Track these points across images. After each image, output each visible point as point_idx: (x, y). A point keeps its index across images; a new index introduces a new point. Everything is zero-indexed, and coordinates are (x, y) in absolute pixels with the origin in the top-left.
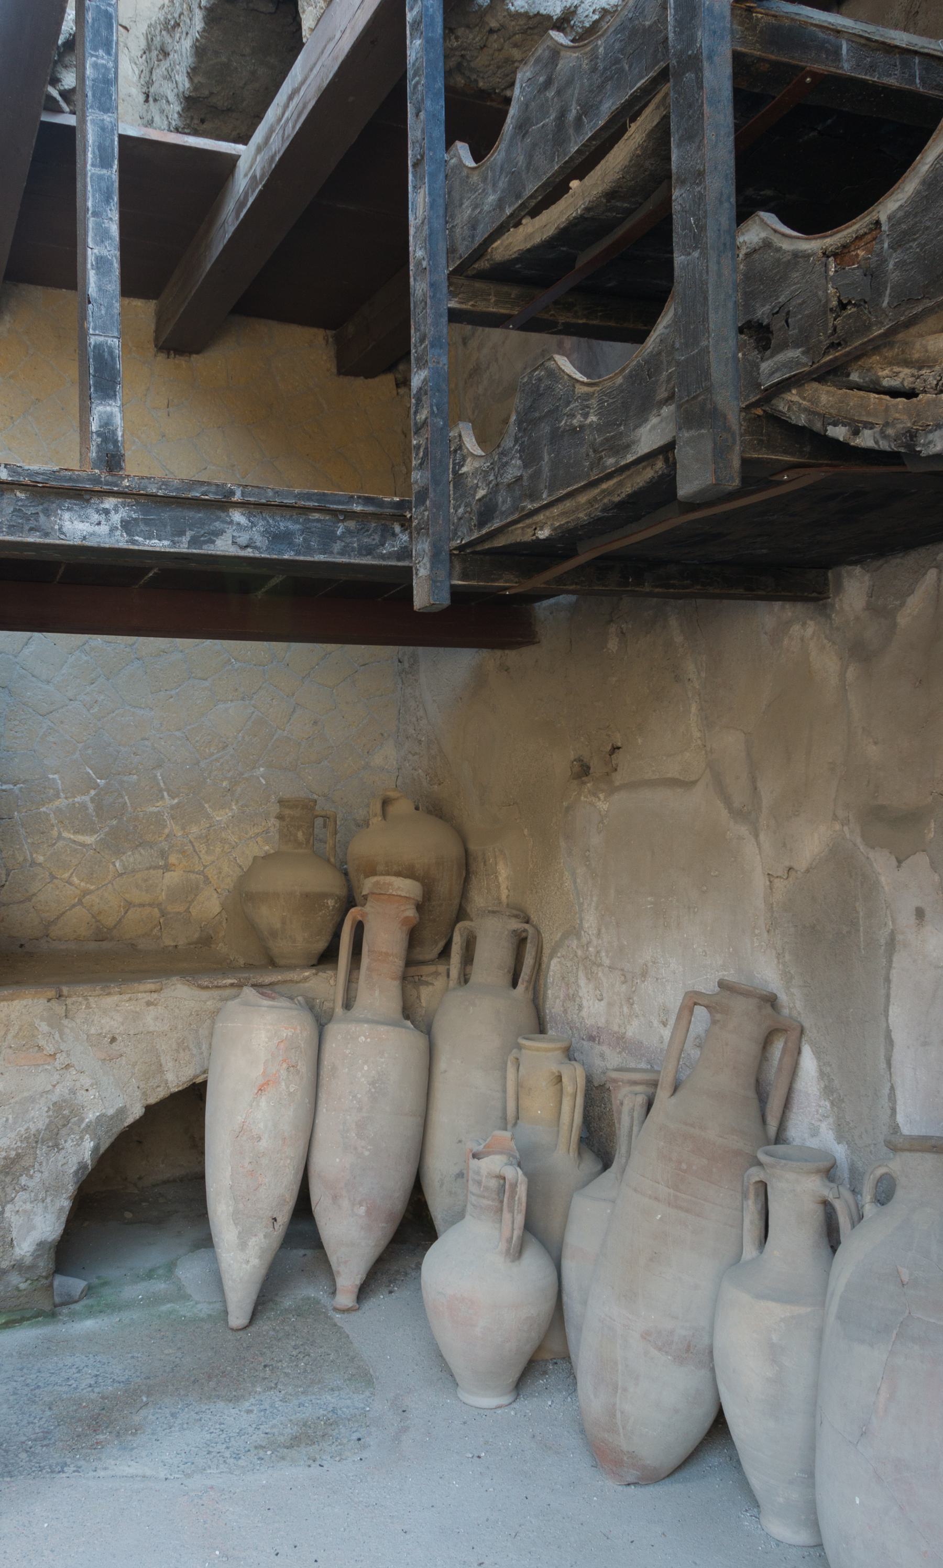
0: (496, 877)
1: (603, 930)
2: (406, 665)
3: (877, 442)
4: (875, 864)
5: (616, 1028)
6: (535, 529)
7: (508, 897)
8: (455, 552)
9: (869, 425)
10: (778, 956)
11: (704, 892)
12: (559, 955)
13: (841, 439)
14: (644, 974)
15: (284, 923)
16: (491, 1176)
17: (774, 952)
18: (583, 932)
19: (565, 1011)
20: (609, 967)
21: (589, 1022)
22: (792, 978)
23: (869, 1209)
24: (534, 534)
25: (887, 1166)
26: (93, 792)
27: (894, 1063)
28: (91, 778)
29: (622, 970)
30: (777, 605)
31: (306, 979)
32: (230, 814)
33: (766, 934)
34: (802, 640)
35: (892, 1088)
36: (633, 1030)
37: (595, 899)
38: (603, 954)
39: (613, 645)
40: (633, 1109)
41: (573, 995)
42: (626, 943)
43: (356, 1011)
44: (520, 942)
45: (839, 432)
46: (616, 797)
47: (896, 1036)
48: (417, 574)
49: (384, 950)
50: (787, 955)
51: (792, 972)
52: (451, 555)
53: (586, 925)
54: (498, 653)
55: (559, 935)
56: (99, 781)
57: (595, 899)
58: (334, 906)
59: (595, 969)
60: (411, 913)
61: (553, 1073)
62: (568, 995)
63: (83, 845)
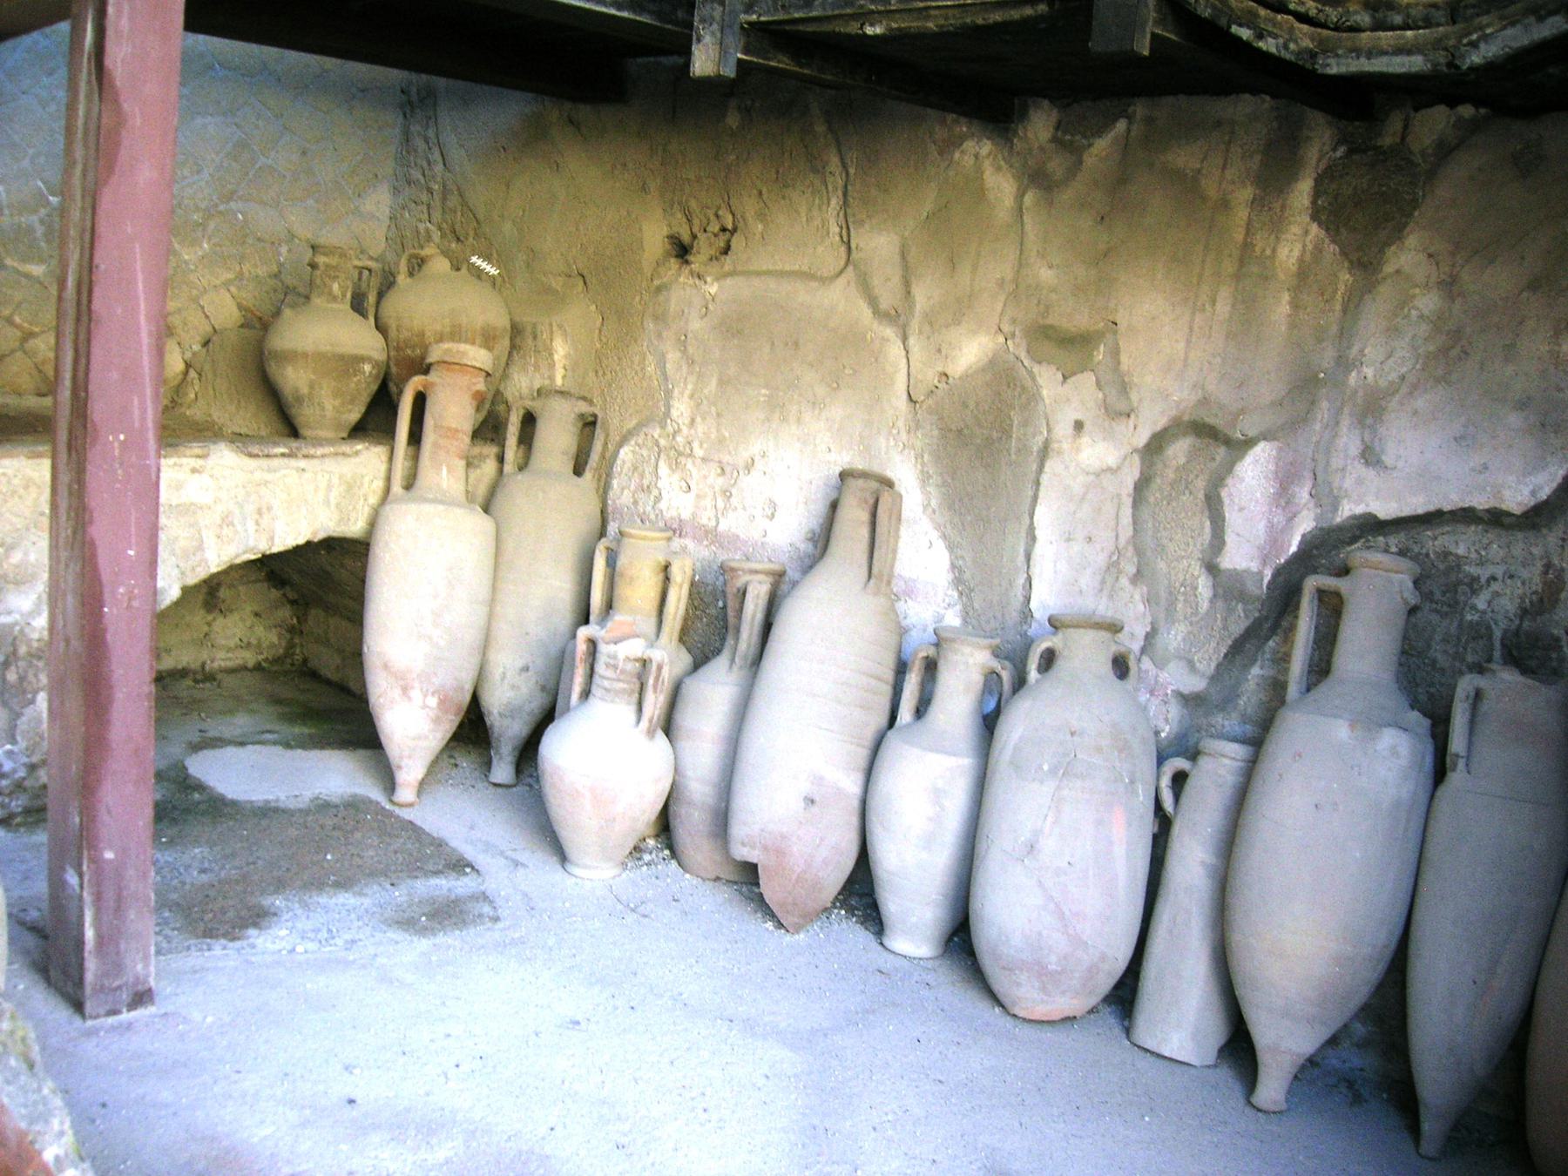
0: (551, 355)
1: (699, 419)
2: (414, 98)
3: (1279, 51)
4: (1038, 378)
5: (704, 521)
6: (862, 25)
7: (564, 377)
8: (746, 26)
9: (1276, 37)
10: (918, 457)
11: (834, 389)
12: (633, 442)
13: (1245, 38)
14: (749, 466)
15: (312, 387)
16: (628, 659)
17: (912, 452)
18: (669, 421)
19: (635, 503)
20: (703, 459)
21: (667, 515)
22: (930, 477)
23: (1033, 675)
24: (861, 28)
25: (1051, 640)
26: (43, 211)
27: (1034, 556)
28: (41, 194)
29: (720, 462)
30: (950, 117)
31: (357, 453)
32: (200, 253)
33: (904, 436)
34: (976, 156)
35: (1029, 580)
36: (731, 524)
37: (690, 387)
38: (696, 445)
39: (733, 120)
40: (758, 596)
41: (648, 487)
42: (727, 435)
43: (415, 492)
44: (589, 425)
45: (1245, 33)
46: (729, 281)
47: (1037, 532)
48: (699, 40)
49: (454, 426)
50: (926, 456)
51: (931, 472)
52: (742, 28)
53: (674, 413)
54: (568, 105)
55: (634, 422)
56: (51, 198)
57: (690, 387)
58: (370, 373)
59: (682, 460)
60: (481, 385)
61: (660, 563)
62: (642, 486)
63: (27, 276)
